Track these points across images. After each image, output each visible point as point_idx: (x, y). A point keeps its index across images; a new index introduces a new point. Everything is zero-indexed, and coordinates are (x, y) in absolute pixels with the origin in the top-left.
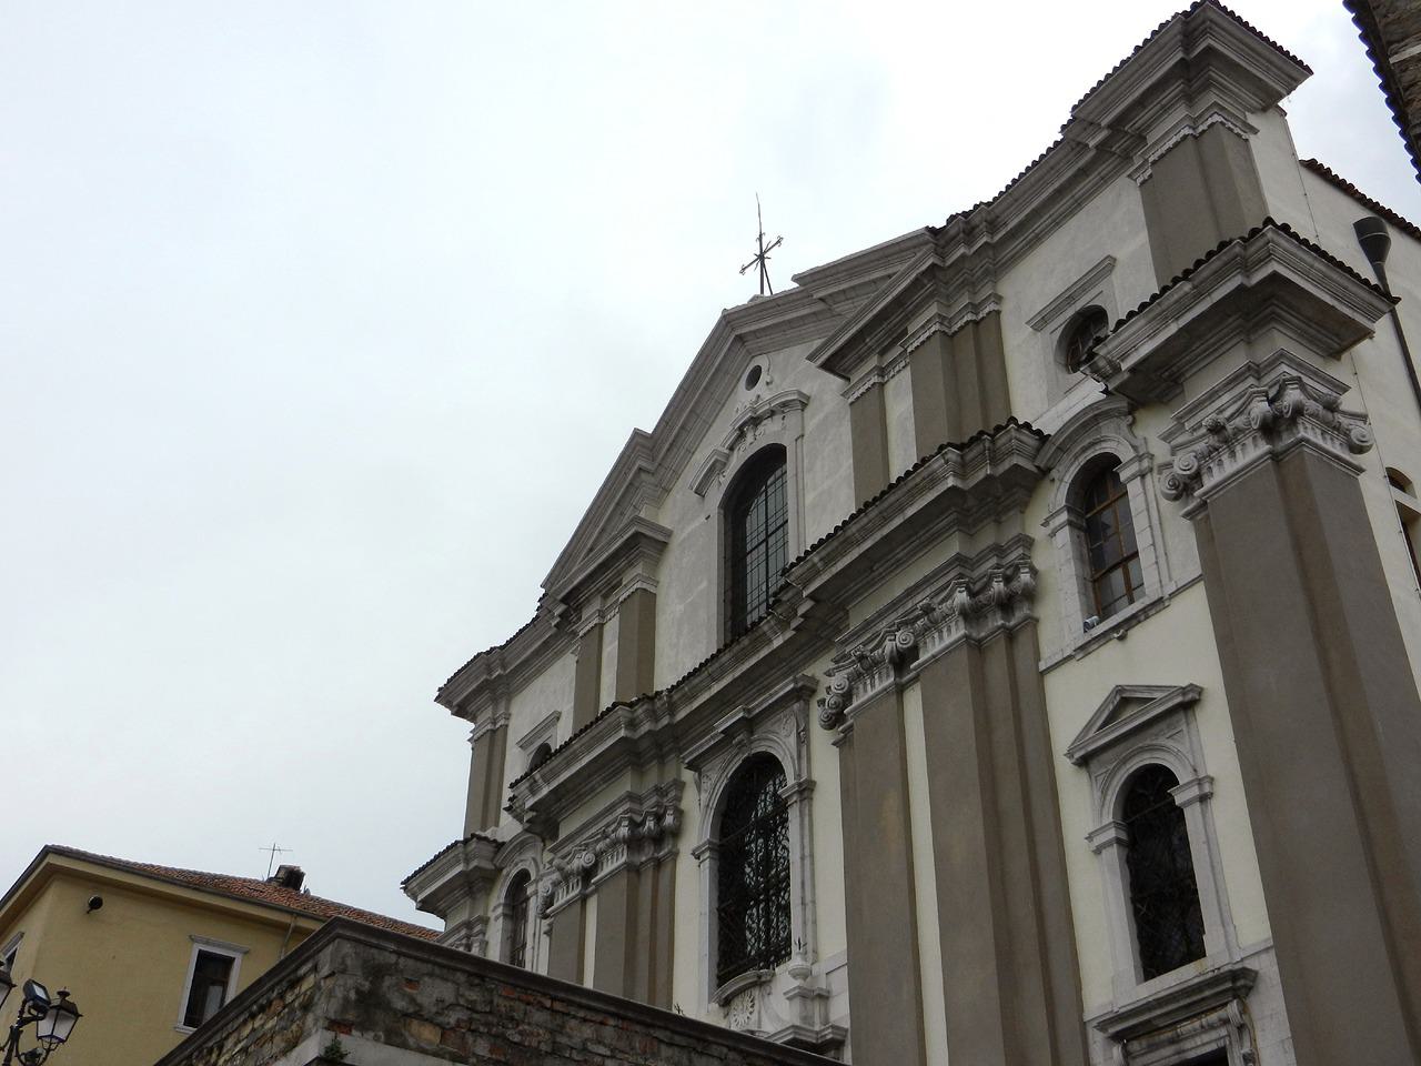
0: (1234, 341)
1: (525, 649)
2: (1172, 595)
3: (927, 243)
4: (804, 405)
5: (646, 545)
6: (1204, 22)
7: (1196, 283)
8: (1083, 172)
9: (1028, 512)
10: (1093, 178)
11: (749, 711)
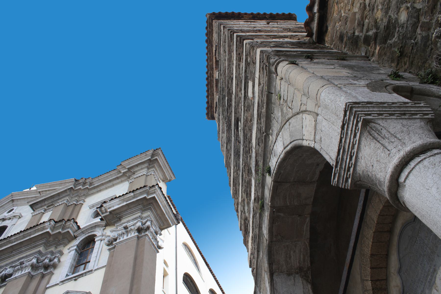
0: (138, 212)
2: (95, 270)
3: (73, 182)
4: (20, 218)
6: (157, 153)
7: (135, 194)
8: (118, 178)
10: (119, 180)
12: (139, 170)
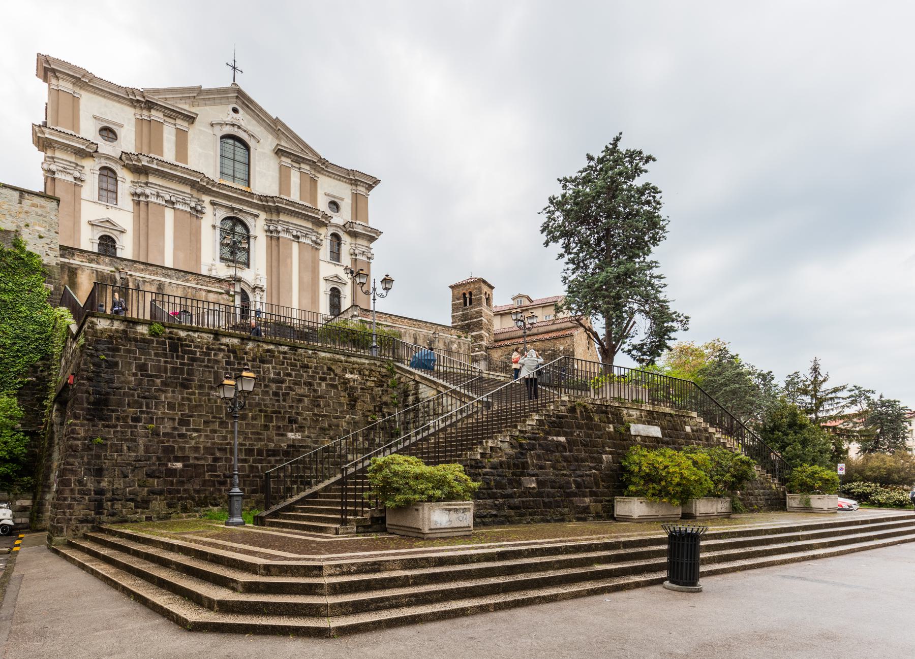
8: (345, 178)
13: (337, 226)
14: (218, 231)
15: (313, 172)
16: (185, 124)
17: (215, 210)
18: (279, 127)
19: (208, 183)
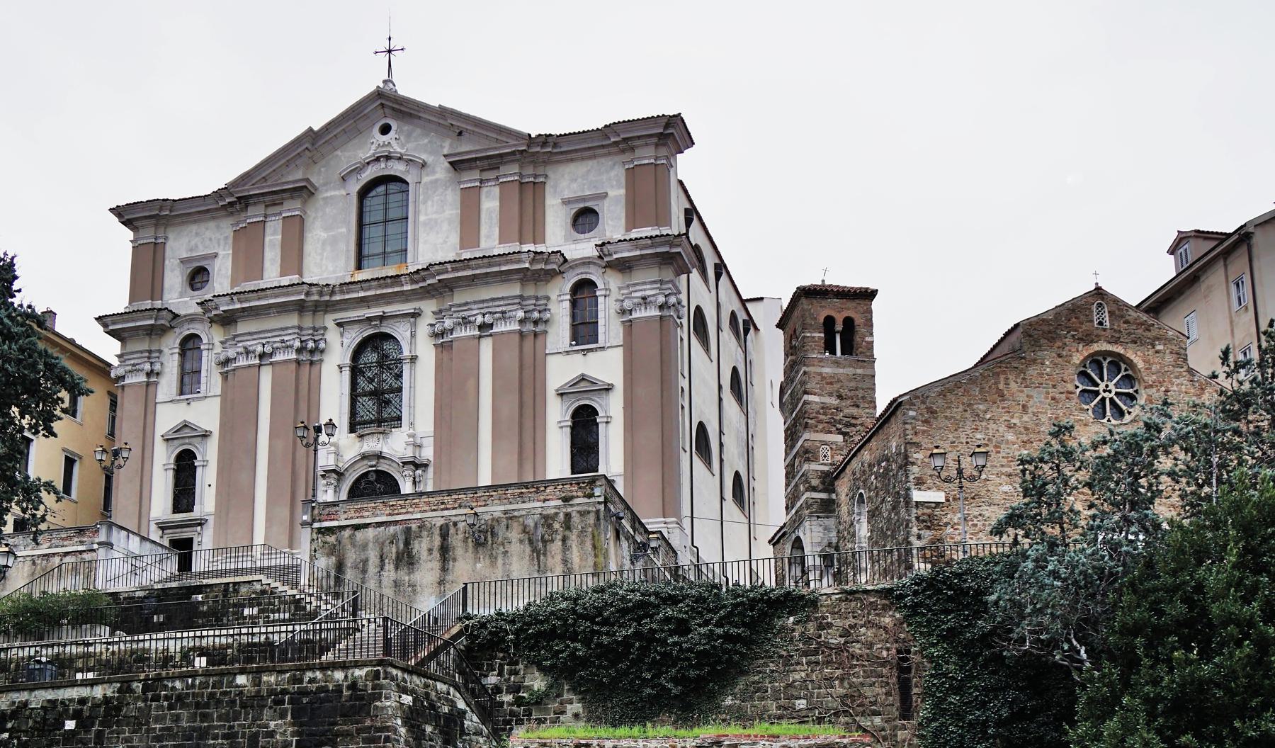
1: (191, 207)
4: (423, 166)
5: (304, 191)
8: (603, 147)
9: (549, 284)
10: (606, 151)
11: (384, 313)
12: (642, 146)
13: (586, 262)
14: (347, 374)
15: (529, 170)
16: (297, 204)
17: (342, 335)
18: (449, 121)
19: (321, 294)
